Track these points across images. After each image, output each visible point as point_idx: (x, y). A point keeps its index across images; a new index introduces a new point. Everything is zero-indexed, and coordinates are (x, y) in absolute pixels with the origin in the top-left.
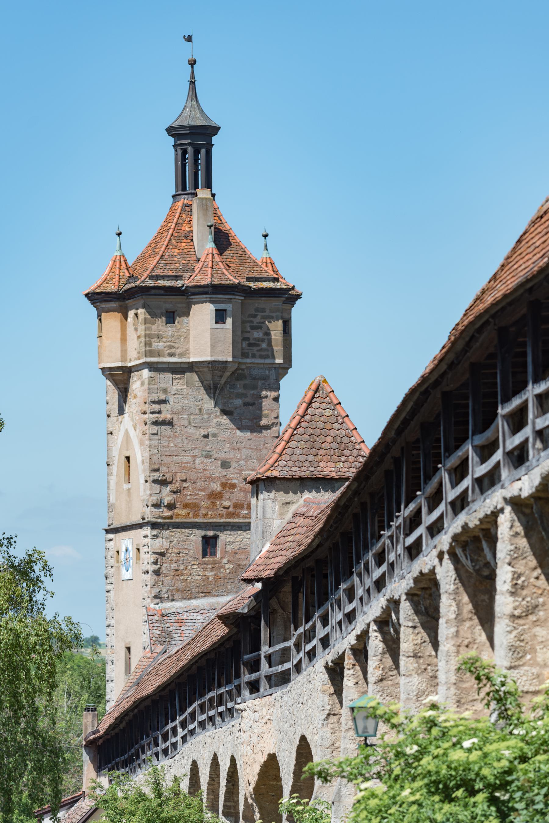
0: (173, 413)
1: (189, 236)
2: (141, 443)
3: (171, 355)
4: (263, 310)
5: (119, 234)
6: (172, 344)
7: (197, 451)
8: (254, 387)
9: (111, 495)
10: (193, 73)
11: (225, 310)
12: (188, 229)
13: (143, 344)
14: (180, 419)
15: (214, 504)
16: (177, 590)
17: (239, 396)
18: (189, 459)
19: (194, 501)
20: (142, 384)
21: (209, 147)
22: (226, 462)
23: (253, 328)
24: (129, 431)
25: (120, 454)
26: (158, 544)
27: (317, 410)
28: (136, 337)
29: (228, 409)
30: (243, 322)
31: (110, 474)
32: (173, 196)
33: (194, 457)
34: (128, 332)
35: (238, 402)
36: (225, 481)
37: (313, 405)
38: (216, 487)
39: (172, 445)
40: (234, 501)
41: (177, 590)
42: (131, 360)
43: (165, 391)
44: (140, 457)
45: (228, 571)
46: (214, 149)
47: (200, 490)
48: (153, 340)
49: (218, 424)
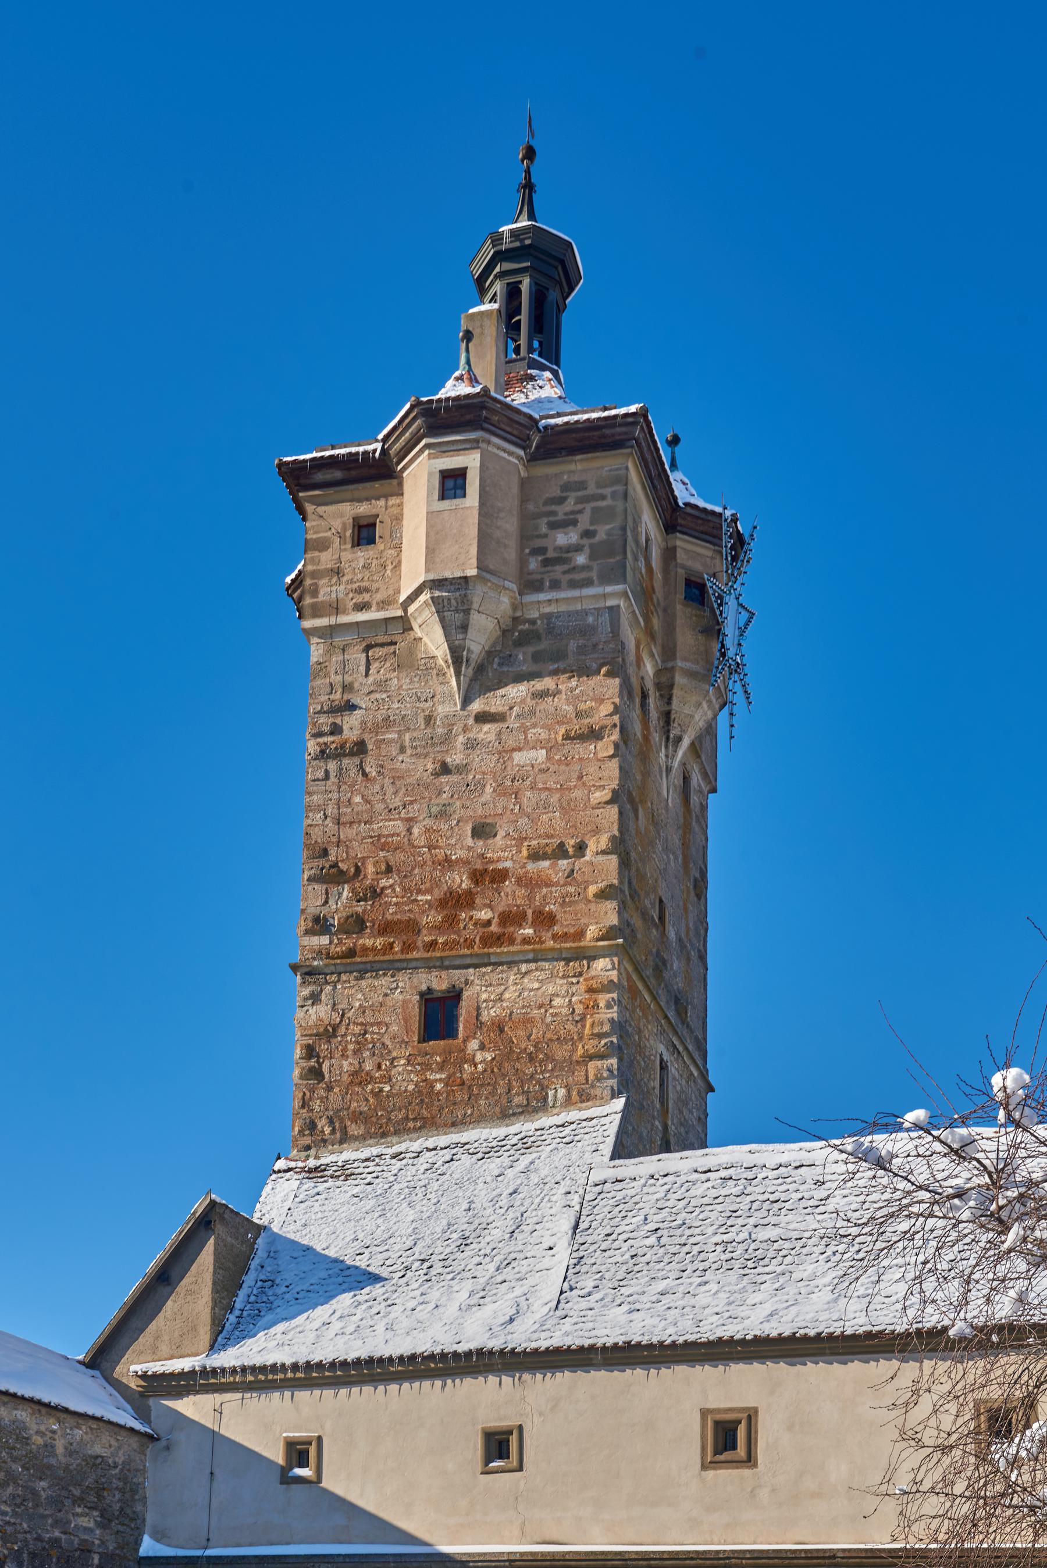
3: (361, 607)
6: (364, 584)
7: (416, 807)
14: (379, 744)
16: (357, 1117)
18: (399, 826)
19: (405, 918)
22: (484, 825)
26: (314, 1017)
29: (493, 710)
38: (461, 880)
39: (358, 799)
40: (501, 909)
41: (357, 1117)
47: (419, 892)
48: (322, 582)
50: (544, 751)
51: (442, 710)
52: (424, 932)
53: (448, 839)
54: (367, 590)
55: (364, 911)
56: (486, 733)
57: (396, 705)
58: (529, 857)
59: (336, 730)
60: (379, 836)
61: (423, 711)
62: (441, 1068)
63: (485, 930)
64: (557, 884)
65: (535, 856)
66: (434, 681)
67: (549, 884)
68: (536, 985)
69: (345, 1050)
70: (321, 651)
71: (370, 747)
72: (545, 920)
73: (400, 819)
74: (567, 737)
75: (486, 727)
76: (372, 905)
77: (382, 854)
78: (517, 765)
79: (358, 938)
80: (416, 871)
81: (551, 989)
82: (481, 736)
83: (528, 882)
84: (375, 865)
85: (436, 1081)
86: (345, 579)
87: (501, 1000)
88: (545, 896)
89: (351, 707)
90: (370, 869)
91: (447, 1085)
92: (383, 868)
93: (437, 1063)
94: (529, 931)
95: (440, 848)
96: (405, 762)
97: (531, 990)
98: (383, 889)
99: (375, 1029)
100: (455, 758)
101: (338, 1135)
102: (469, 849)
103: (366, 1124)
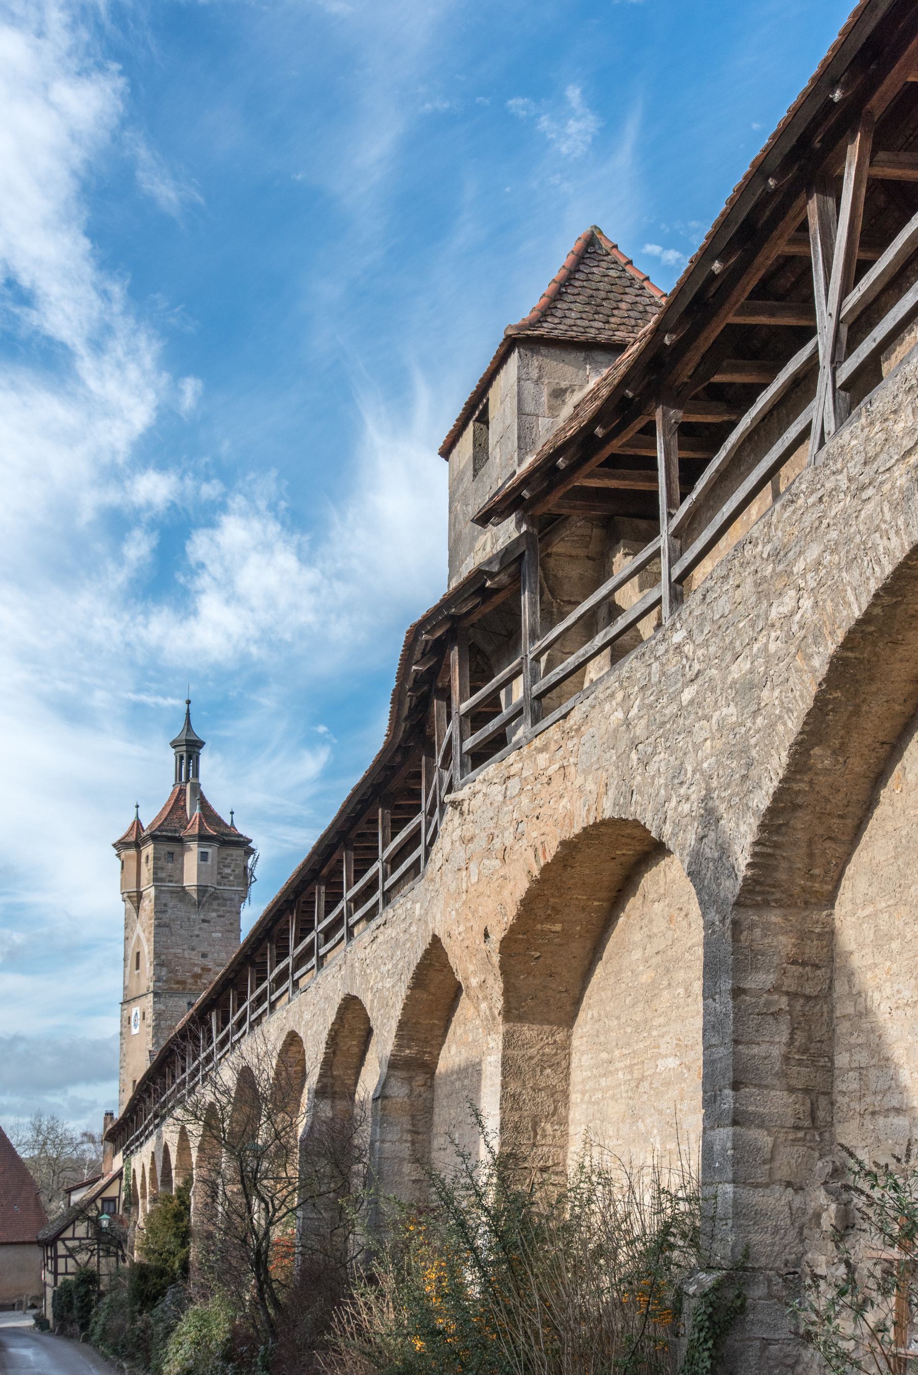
0: (170, 920)
2: (148, 940)
3: (171, 881)
4: (232, 855)
8: (225, 905)
11: (207, 853)
15: (196, 982)
17: (214, 910)
18: (180, 951)
20: (150, 901)
23: (224, 866)
30: (219, 862)
35: (214, 914)
38: (198, 970)
43: (165, 905)
49: (200, 929)
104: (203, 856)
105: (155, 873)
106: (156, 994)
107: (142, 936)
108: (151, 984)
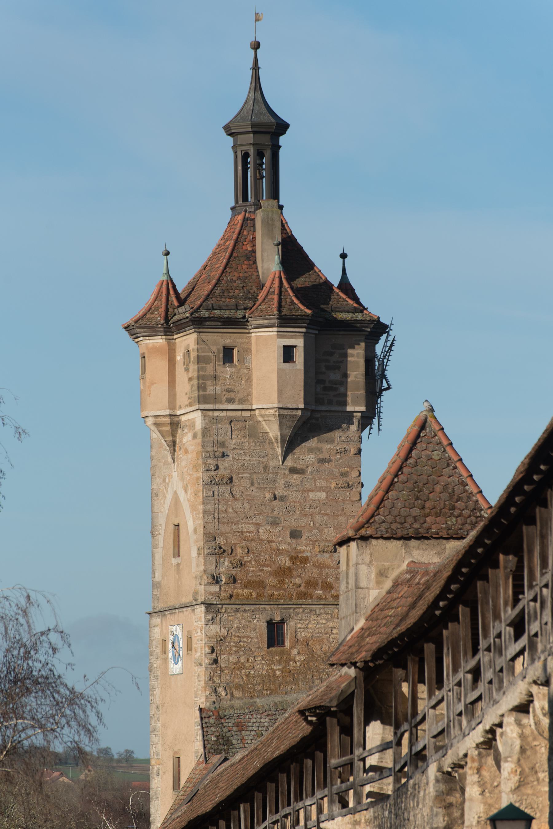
1: (251, 257)
2: (193, 508)
5: (167, 254)
6: (230, 387)
7: (261, 517)
9: (156, 571)
10: (256, 58)
12: (249, 249)
13: (195, 387)
14: (240, 479)
16: (238, 687)
20: (195, 436)
21: (276, 148)
23: (329, 368)
24: (178, 493)
25: (167, 522)
26: (214, 631)
27: (423, 453)
28: (187, 379)
29: (298, 467)
31: (154, 546)
32: (233, 209)
33: (258, 525)
34: (177, 373)
35: (311, 458)
36: (294, 554)
37: (418, 446)
38: (285, 561)
39: (230, 510)
40: (306, 578)
41: (238, 687)
42: (180, 408)
43: (222, 444)
44: (192, 524)
45: (298, 664)
46: (282, 152)
47: (264, 565)
48: (208, 383)
50: (324, 493)
51: (272, 463)
52: (268, 588)
53: (278, 537)
54: (233, 391)
55: (237, 574)
56: (295, 479)
57: (248, 458)
58: (319, 552)
59: (217, 468)
60: (242, 532)
61: (263, 463)
62: (279, 663)
63: (298, 589)
64: (333, 567)
65: (322, 551)
66: (267, 446)
67: (329, 567)
68: (324, 622)
69: (230, 650)
70: (207, 421)
71: (234, 480)
72: (328, 586)
73: (253, 523)
74: (336, 487)
75: (295, 476)
76: (241, 571)
77: (245, 543)
78: (311, 499)
79: (235, 588)
80: (263, 553)
81: (331, 625)
82: (293, 481)
83: (320, 566)
84: (242, 547)
85: (277, 670)
86: (221, 382)
87: (307, 628)
88: (327, 574)
89: (224, 455)
90: (239, 551)
91: (282, 672)
92: (246, 551)
93: (277, 660)
94: (321, 592)
95: (274, 542)
96: (254, 492)
97: (322, 624)
98: (245, 562)
99: (245, 640)
100: (280, 492)
101: (229, 696)
102: (289, 544)
103: (243, 692)
104: (288, 354)
105: (201, 387)
106: (208, 606)
107: (182, 495)
108: (202, 589)
